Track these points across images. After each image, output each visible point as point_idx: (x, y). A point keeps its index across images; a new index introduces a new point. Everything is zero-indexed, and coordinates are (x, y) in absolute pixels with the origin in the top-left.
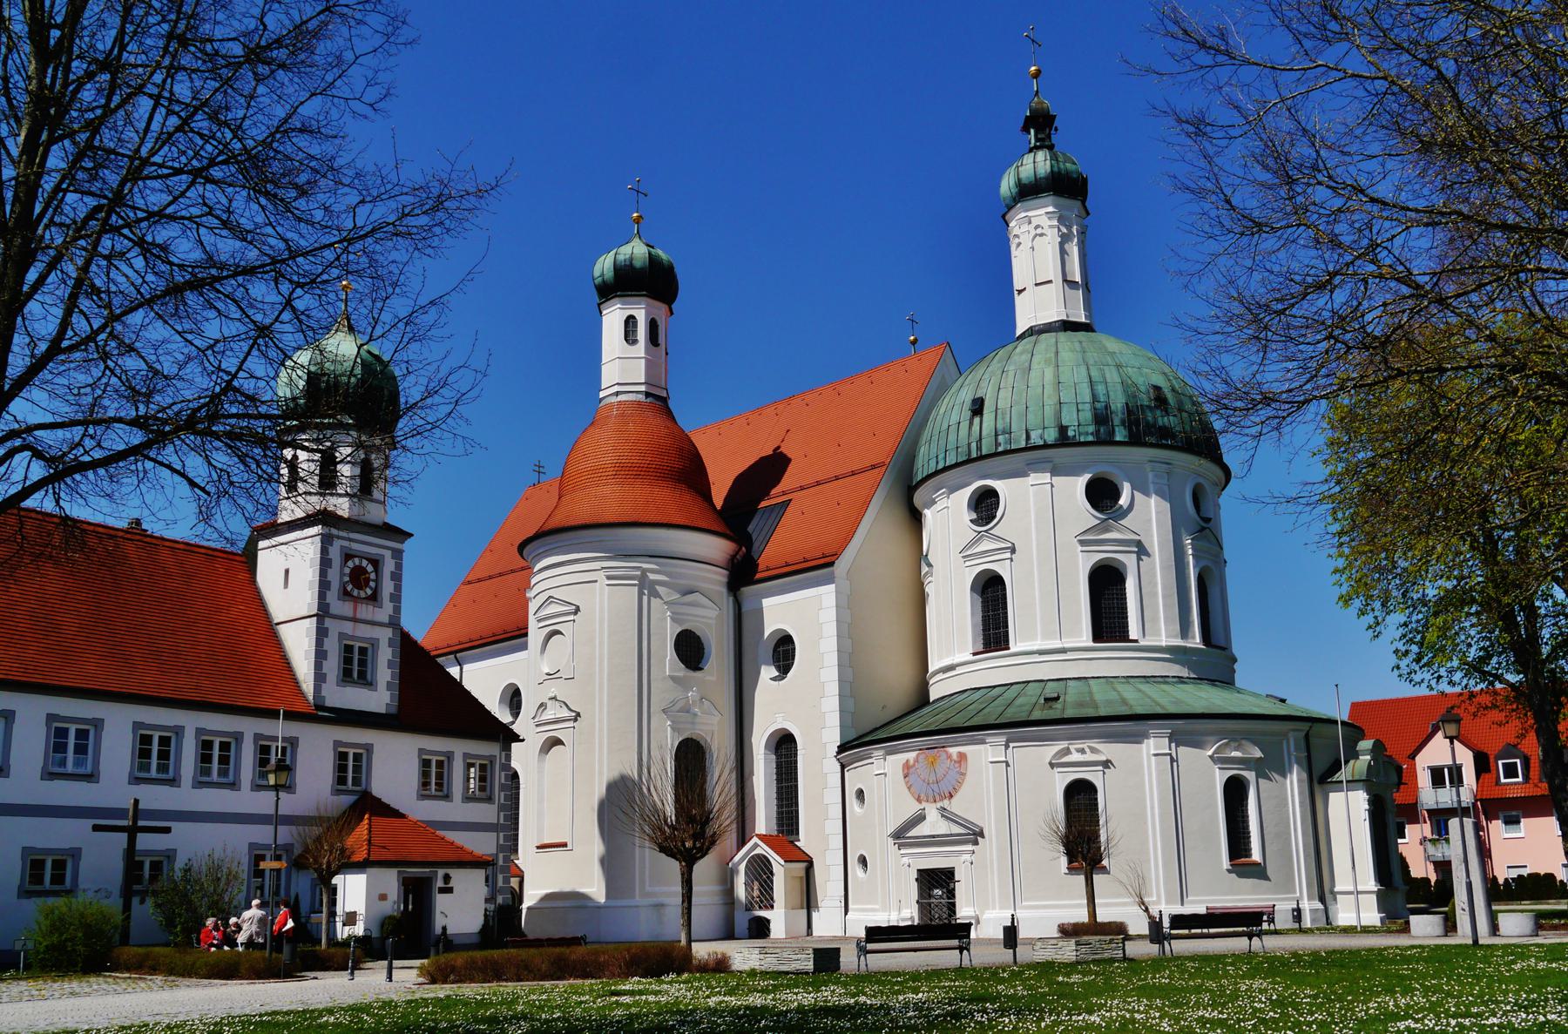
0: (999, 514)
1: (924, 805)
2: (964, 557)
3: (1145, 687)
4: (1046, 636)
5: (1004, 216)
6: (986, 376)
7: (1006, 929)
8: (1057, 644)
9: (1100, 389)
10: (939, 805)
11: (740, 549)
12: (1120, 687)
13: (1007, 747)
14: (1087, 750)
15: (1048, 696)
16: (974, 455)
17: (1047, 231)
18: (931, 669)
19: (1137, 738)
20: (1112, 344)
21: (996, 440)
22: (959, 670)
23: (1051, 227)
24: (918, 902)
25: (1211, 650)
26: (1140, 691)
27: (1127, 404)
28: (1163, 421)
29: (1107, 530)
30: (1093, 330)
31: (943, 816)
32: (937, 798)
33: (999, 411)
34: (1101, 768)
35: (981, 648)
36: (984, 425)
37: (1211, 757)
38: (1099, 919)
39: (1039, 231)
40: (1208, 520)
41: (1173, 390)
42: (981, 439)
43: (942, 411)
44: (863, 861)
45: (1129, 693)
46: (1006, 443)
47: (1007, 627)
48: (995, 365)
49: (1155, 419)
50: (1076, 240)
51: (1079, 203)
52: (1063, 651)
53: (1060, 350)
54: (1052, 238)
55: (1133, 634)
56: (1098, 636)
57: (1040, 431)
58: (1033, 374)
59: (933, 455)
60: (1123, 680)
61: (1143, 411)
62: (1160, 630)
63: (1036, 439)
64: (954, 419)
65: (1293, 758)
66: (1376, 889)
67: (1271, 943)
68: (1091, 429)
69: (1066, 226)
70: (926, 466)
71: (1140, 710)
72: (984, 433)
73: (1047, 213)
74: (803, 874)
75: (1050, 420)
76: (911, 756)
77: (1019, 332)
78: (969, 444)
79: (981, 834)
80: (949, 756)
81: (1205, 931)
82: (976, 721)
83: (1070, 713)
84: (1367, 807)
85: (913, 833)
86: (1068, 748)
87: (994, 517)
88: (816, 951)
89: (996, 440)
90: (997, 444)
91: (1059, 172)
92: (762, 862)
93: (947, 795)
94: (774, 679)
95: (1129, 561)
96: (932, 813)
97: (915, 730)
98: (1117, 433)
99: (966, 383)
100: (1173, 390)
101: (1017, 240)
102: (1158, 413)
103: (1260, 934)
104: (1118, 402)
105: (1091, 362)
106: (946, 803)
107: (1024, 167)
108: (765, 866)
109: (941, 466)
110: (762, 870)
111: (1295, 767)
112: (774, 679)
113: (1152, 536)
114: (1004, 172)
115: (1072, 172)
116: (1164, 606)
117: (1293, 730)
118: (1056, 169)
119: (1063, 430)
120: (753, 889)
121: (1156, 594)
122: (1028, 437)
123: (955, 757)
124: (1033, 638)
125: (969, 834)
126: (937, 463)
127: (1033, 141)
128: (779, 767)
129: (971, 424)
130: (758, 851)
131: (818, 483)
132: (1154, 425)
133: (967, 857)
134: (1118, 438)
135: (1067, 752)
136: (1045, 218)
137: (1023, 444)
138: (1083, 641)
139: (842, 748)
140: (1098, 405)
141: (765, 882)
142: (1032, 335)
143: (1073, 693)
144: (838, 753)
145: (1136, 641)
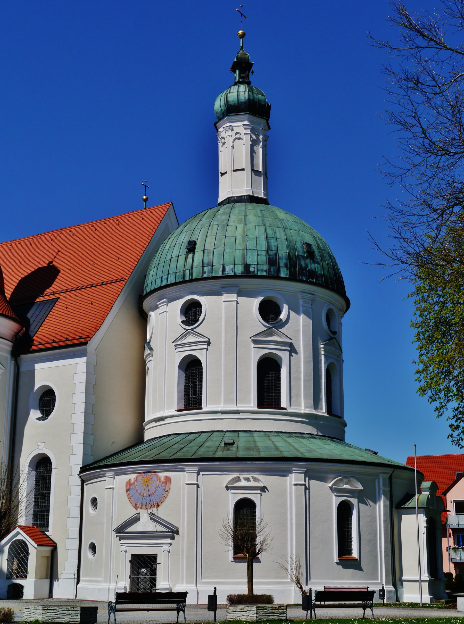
0: (201, 318)
1: (139, 510)
2: (175, 345)
3: (290, 440)
4: (227, 401)
5: (215, 124)
6: (199, 227)
7: (210, 597)
8: (233, 407)
9: (273, 242)
10: (149, 511)
11: (22, 329)
12: (274, 439)
13: (198, 474)
14: (251, 479)
15: (227, 442)
16: (187, 278)
17: (243, 136)
18: (147, 419)
19: (284, 473)
20: (281, 214)
21: (203, 269)
22: (167, 421)
23: (246, 134)
24: (130, 577)
25: (331, 417)
26: (286, 442)
27: (289, 253)
28: (311, 266)
29: (271, 335)
30: (268, 204)
31: (151, 519)
32: (149, 506)
33: (206, 251)
34: (259, 491)
35: (182, 407)
36: (196, 259)
37: (331, 488)
38: (255, 593)
39: (238, 136)
40: (334, 333)
41: (318, 247)
42: (192, 268)
43: (167, 247)
44: (93, 547)
45: (279, 443)
46: (209, 272)
47: (201, 394)
48: (205, 220)
49: (306, 263)
50: (261, 144)
51: (264, 121)
52: (238, 412)
53: (248, 214)
54: (246, 141)
55: (284, 403)
56: (260, 404)
57: (232, 266)
58: (229, 228)
59: (159, 276)
60: (276, 434)
61: (299, 259)
62: (300, 402)
63: (229, 271)
64: (175, 253)
65: (381, 491)
66: (428, 579)
67: (379, 612)
68: (265, 267)
69: (255, 135)
70: (154, 283)
71: (287, 454)
72: (195, 264)
73: (244, 125)
74: (49, 554)
75: (239, 260)
76: (133, 477)
77: (220, 200)
78: (184, 271)
79: (177, 532)
80: (159, 479)
81: (323, 603)
82: (178, 456)
83: (241, 454)
84: (425, 525)
85: (130, 529)
86: (239, 477)
87: (198, 320)
88: (83, 609)
89: (203, 269)
90: (203, 273)
91: (253, 100)
92: (21, 545)
93: (156, 504)
94: (39, 419)
95: (284, 356)
96: (144, 516)
97: (137, 460)
98: (282, 272)
99: (185, 230)
100: (318, 247)
101: (223, 141)
102: (308, 261)
103: (371, 607)
104: (283, 252)
105: (268, 224)
106: (154, 510)
107: (231, 94)
108: (23, 548)
109: (164, 283)
110: (21, 551)
111: (383, 497)
112: (39, 419)
113: (299, 341)
114: (217, 96)
115: (261, 101)
116: (305, 387)
117: (382, 473)
118: (251, 98)
119: (247, 267)
120: (13, 564)
121: (299, 379)
122: (224, 270)
123: (162, 479)
124: (218, 402)
125: (168, 532)
126: (162, 281)
127: (237, 78)
128: (37, 479)
129: (187, 257)
130: (19, 537)
131: (78, 289)
132: (305, 269)
133: (166, 547)
134: (282, 275)
135: (238, 479)
136: (242, 128)
137: (220, 274)
138: (251, 407)
139: (83, 469)
140: (271, 253)
141: (22, 559)
142: (229, 203)
143: (242, 441)
144: (81, 472)
145: (285, 409)
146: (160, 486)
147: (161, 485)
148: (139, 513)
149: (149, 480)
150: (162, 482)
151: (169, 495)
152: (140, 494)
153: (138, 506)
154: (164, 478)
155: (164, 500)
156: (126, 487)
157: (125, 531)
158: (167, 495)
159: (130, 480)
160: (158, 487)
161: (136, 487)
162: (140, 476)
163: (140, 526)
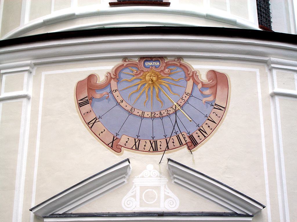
1: (126, 154)
10: (168, 155)
80: (193, 76)
123: (203, 78)
146: (196, 93)
148: (128, 160)
149: (158, 78)
150: (203, 85)
152: (130, 113)
153: (122, 142)
154: (207, 75)
155: (213, 130)
157: (73, 212)
159: (91, 77)
160: (191, 95)
161: (116, 94)
163: (134, 196)
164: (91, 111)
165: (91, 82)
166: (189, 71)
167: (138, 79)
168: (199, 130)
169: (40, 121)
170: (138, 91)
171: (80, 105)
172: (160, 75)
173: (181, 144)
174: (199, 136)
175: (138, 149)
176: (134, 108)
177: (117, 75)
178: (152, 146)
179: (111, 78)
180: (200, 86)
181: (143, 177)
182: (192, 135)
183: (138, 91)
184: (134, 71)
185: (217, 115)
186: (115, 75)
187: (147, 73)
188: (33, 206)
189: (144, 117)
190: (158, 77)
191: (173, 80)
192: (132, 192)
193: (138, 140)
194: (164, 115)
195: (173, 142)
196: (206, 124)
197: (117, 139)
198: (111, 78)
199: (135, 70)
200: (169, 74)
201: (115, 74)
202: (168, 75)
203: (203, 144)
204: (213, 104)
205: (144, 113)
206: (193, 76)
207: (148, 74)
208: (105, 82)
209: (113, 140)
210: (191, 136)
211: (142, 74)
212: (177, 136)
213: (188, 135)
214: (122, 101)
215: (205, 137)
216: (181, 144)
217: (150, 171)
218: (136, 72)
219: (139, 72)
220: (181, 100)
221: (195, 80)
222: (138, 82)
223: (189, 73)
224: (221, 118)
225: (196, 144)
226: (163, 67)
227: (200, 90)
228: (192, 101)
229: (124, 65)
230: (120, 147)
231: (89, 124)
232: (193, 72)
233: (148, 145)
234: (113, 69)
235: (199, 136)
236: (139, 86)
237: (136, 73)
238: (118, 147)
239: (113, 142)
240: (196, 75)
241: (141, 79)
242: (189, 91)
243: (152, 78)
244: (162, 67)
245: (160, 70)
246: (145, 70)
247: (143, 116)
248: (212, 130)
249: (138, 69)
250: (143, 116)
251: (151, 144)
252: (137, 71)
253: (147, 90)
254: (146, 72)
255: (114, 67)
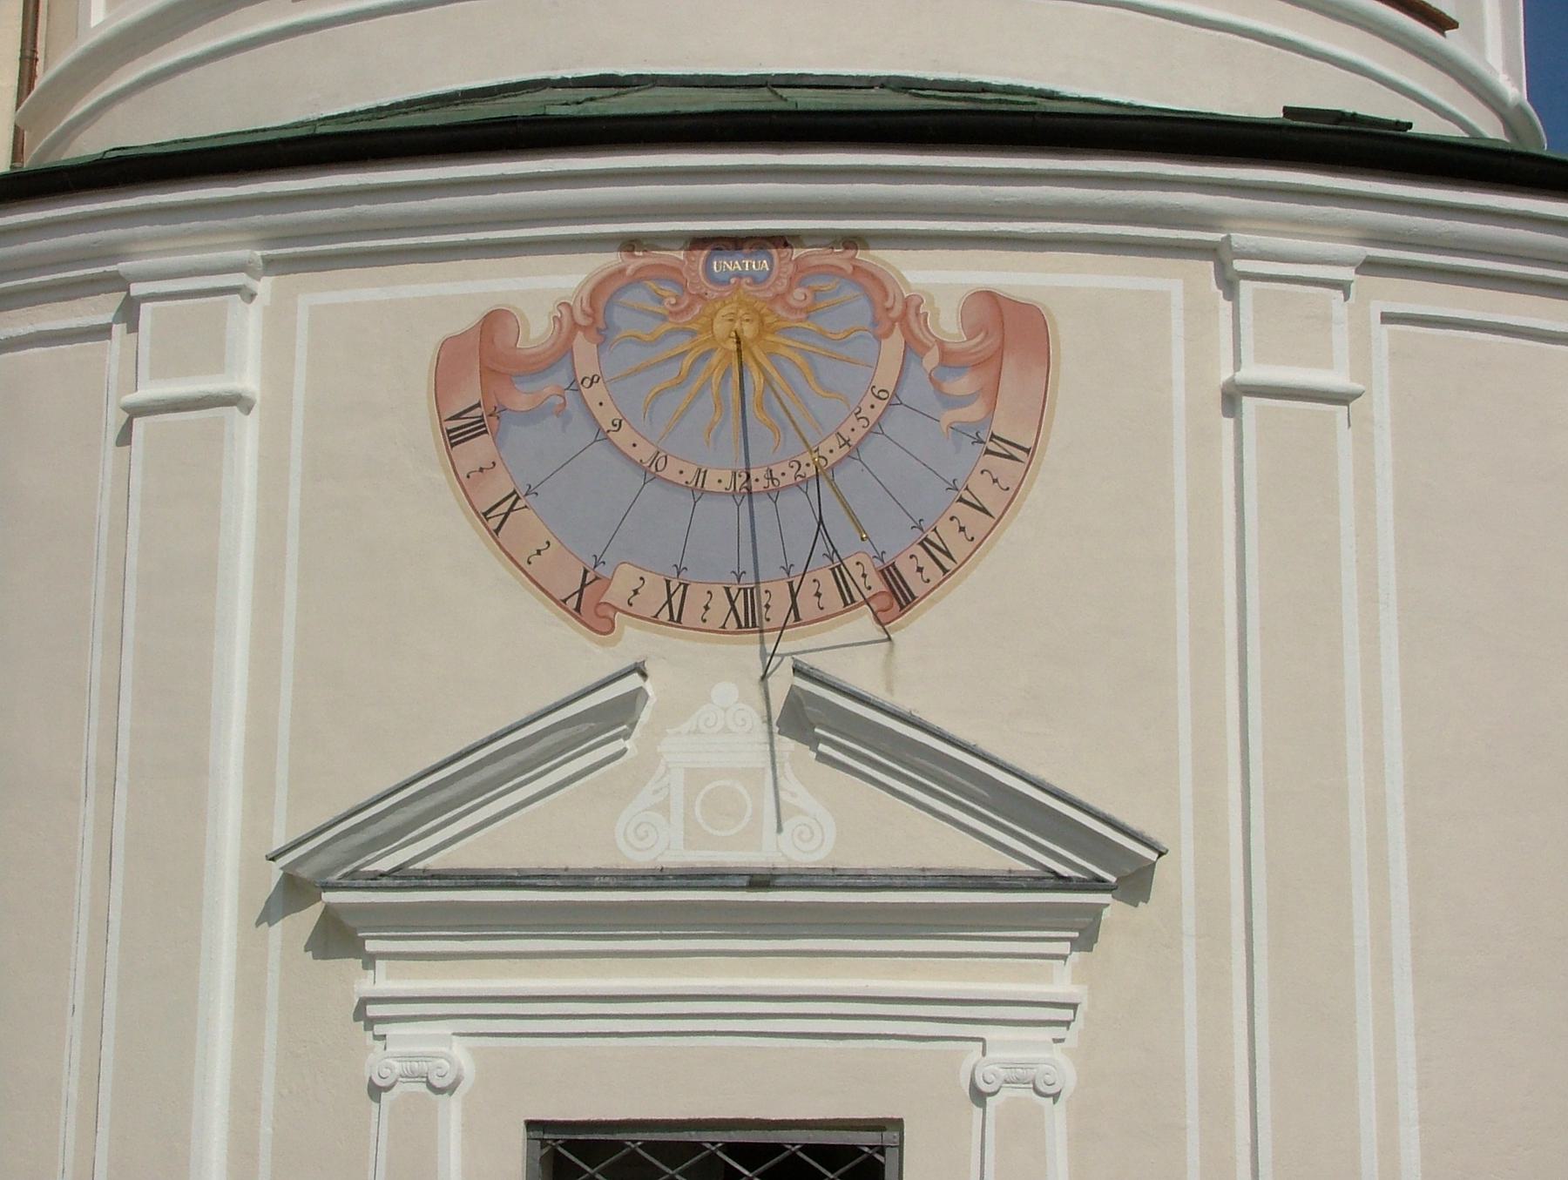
1: (633, 640)
123: (948, 324)
146: (917, 390)
147: (936, 383)
149: (763, 328)
150: (945, 354)
151: (1036, 495)
152: (650, 473)
153: (618, 592)
154: (964, 314)
155: (976, 543)
156: (440, 392)
157: (433, 863)
158: (1012, 495)
159: (494, 322)
160: (893, 400)
161: (593, 394)
162: (638, 278)
163: (664, 808)
164: (494, 464)
165: (493, 340)
166: (891, 295)
167: (683, 331)
168: (921, 544)
169: (294, 503)
170: (681, 382)
171: (450, 439)
172: (772, 312)
173: (848, 601)
174: (920, 570)
175: (679, 620)
176: (663, 454)
177: (600, 316)
178: (734, 609)
179: (575, 326)
180: (932, 359)
181: (697, 732)
182: (893, 565)
183: (681, 382)
184: (666, 298)
185: (995, 481)
186: (589, 316)
187: (717, 306)
188: (278, 844)
189: (703, 492)
190: (762, 322)
191: (822, 334)
192: (656, 792)
193: (680, 584)
194: (784, 482)
195: (818, 595)
196: (952, 519)
197: (597, 578)
198: (575, 326)
199: (669, 292)
200: (808, 312)
201: (589, 310)
202: (803, 316)
203: (933, 602)
204: (984, 436)
205: (706, 472)
206: (904, 314)
207: (724, 311)
208: (551, 342)
209: (583, 585)
210: (887, 568)
211: (697, 312)
212: (833, 570)
213: (879, 564)
214: (617, 422)
215: (945, 571)
216: (848, 601)
217: (725, 710)
218: (673, 301)
219: (686, 301)
220: (852, 420)
221: (911, 331)
222: (683, 343)
223: (888, 304)
224: (1011, 493)
225: (908, 602)
226: (785, 281)
227: (931, 378)
228: (897, 423)
229: (629, 272)
230: (611, 614)
231: (487, 519)
232: (906, 302)
233: (721, 605)
234: (581, 287)
235: (920, 570)
236: (688, 361)
237: (676, 304)
238: (601, 611)
239: (581, 592)
240: (917, 314)
241: (693, 333)
242: (886, 378)
243: (737, 325)
244: (778, 278)
245: (770, 295)
246: (713, 292)
247: (700, 484)
248: (976, 542)
249: (684, 287)
250: (700, 484)
251: (732, 602)
252: (676, 297)
253: (716, 379)
254: (716, 301)
255: (587, 281)
